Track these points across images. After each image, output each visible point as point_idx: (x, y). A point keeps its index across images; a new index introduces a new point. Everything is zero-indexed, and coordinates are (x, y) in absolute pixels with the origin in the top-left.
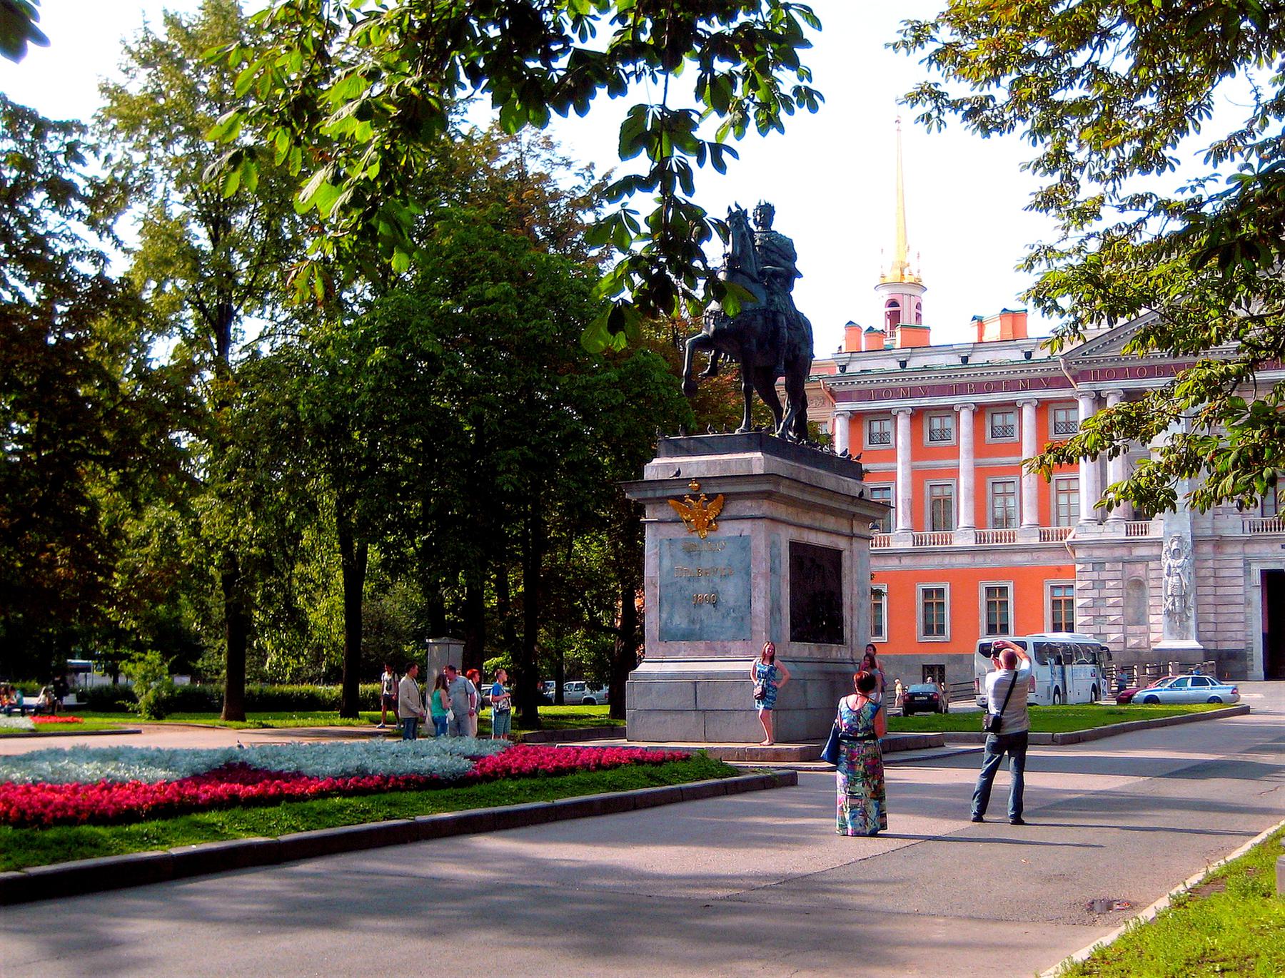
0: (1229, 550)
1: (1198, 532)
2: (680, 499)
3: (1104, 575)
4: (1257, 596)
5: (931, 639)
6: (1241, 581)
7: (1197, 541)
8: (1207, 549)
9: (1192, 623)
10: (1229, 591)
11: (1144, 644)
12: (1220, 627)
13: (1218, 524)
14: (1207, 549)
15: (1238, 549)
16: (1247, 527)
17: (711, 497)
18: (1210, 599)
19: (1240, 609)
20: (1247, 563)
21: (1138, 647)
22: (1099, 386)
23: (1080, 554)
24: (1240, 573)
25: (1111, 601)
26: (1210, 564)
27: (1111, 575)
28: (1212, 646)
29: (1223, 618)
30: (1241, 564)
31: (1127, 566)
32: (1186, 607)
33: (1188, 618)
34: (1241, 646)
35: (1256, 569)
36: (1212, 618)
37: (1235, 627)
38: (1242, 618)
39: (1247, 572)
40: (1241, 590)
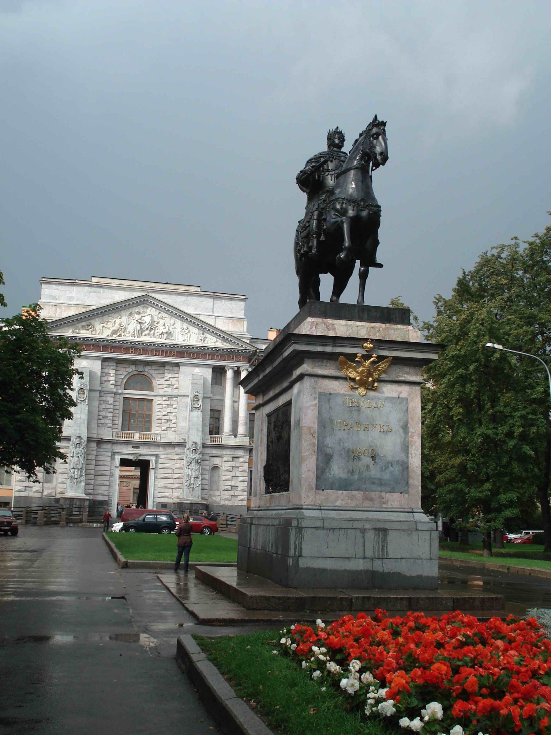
0: (104, 446)
1: (90, 436)
2: (351, 357)
6: (109, 464)
7: (89, 440)
10: (102, 468)
11: (53, 494)
13: (100, 432)
14: (94, 445)
15: (109, 446)
16: (114, 436)
17: (381, 358)
18: (93, 472)
21: (49, 495)
24: (109, 459)
28: (91, 497)
30: (110, 454)
34: (106, 498)
35: (117, 458)
36: (92, 482)
37: (104, 488)
38: (108, 484)
39: (113, 459)
40: (108, 468)
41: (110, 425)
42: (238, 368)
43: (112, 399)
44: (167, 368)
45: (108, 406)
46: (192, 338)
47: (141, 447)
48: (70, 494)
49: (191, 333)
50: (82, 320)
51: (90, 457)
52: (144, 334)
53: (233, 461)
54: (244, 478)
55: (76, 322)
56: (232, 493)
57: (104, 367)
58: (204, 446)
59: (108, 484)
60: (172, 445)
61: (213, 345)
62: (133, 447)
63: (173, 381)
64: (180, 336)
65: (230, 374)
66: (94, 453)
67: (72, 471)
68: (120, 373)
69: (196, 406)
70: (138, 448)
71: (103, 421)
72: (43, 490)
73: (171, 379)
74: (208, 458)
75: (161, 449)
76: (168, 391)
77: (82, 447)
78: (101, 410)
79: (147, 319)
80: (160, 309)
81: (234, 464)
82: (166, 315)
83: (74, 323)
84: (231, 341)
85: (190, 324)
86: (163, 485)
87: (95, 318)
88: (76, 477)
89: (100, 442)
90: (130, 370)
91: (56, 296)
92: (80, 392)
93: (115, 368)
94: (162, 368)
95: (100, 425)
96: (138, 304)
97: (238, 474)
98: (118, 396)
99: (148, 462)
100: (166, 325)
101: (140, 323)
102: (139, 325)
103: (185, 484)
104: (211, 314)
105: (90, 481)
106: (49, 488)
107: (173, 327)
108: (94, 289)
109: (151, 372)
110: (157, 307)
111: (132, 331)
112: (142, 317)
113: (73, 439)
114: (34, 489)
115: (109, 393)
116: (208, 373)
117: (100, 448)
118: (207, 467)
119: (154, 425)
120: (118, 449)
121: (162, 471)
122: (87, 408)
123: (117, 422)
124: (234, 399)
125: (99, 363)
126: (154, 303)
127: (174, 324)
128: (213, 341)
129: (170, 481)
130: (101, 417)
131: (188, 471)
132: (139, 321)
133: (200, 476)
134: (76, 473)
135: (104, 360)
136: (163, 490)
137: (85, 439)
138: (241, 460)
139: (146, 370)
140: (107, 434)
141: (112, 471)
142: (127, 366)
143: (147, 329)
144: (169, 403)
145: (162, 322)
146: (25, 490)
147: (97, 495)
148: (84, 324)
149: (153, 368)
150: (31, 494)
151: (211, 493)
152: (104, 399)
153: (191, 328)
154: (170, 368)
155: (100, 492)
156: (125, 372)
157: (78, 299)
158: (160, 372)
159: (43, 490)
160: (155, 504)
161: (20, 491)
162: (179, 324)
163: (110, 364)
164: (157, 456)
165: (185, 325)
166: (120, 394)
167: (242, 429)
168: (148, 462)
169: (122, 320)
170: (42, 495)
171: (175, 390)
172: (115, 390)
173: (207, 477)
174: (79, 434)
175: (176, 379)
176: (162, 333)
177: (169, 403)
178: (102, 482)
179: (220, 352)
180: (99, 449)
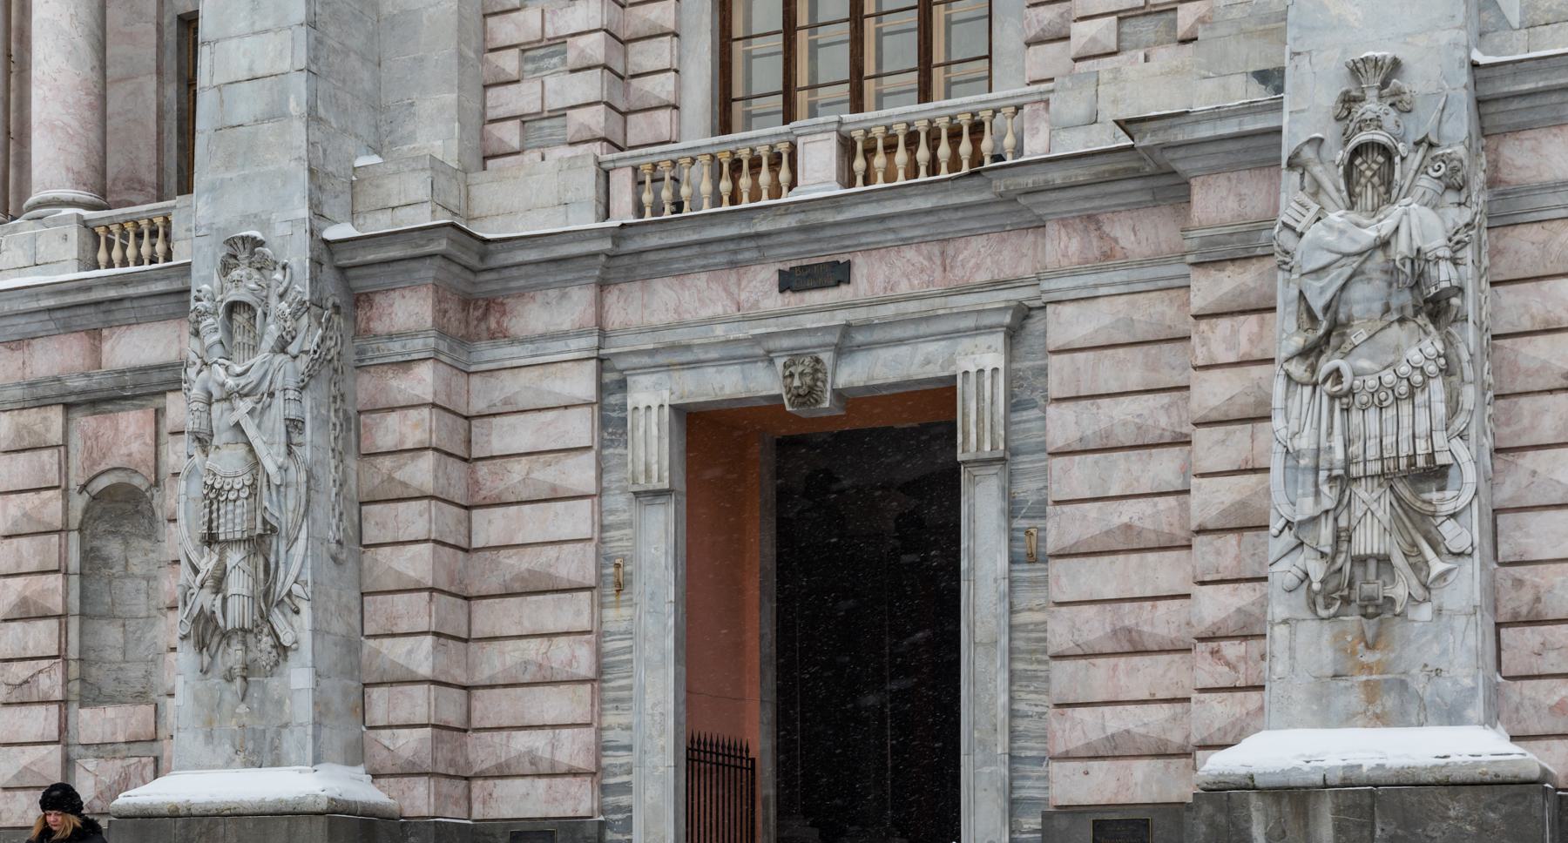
0: (533, 316)
4: (655, 541)
6: (580, 473)
10: (532, 523)
19: (574, 612)
24: (579, 428)
26: (423, 381)
29: (495, 662)
30: (582, 383)
35: (651, 398)
39: (612, 423)
40: (575, 520)
47: (861, 267)
62: (789, 282)
70: (839, 274)
99: (939, 399)
103: (1284, 572)
131: (1299, 421)
133: (1466, 459)
140: (539, 198)
141: (618, 543)
164: (1019, 326)
168: (939, 399)
174: (247, 219)
178: (533, 648)
180: (490, 354)
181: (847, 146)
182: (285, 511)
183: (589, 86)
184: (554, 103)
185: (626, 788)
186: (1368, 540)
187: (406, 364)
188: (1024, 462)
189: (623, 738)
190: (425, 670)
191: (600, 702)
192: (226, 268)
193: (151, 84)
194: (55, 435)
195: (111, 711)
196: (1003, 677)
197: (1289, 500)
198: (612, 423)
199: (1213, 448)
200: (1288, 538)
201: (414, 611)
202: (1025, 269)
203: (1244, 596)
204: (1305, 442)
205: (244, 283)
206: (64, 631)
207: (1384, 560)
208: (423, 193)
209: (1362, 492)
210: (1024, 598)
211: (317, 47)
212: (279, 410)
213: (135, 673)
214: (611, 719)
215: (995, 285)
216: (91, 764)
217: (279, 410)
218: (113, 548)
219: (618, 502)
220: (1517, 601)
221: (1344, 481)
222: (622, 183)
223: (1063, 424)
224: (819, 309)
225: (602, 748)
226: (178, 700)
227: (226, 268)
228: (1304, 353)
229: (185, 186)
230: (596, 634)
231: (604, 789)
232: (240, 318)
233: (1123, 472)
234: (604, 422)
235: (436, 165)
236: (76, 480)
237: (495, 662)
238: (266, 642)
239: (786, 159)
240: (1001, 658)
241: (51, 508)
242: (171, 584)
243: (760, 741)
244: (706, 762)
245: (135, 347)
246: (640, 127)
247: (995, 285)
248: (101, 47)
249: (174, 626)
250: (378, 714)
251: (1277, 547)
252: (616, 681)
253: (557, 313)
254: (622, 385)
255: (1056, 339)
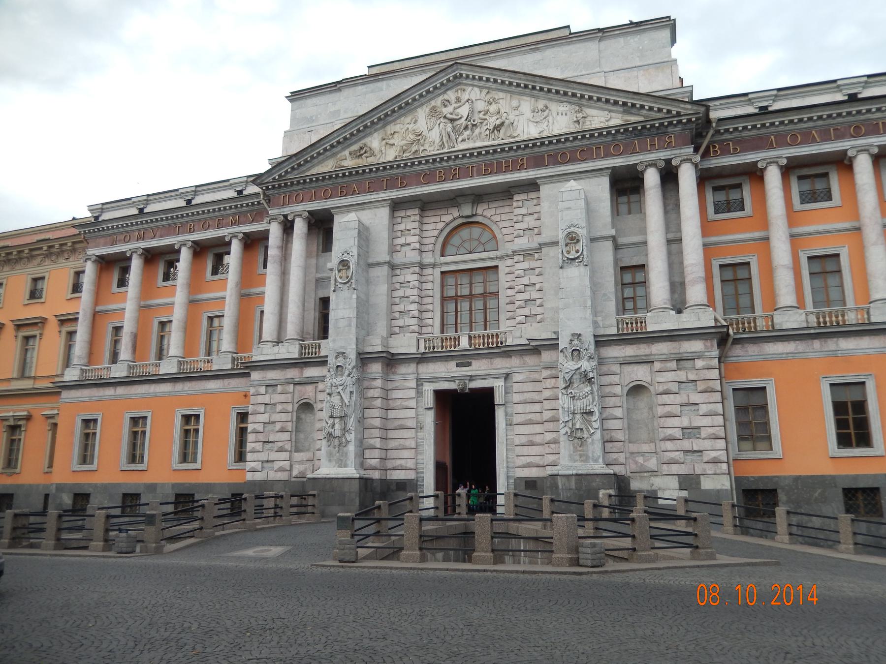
0: (403, 369)
3: (277, 398)
4: (429, 419)
5: (133, 467)
6: (412, 403)
7: (364, 359)
8: (376, 368)
9: (351, 448)
12: (392, 454)
14: (376, 368)
15: (411, 368)
19: (410, 433)
20: (420, 382)
21: (302, 475)
22: (286, 210)
23: (255, 375)
24: (412, 393)
25: (278, 426)
27: (282, 398)
28: (376, 475)
29: (392, 444)
30: (413, 384)
31: (298, 387)
32: (345, 430)
33: (348, 442)
34: (411, 475)
35: (429, 389)
37: (406, 454)
38: (413, 446)
39: (419, 393)
40: (411, 413)
41: (416, 328)
42: (668, 161)
43: (416, 277)
44: (516, 198)
45: (409, 292)
46: (560, 120)
47: (474, 363)
48: (327, 470)
49: (555, 114)
50: (348, 142)
51: (371, 393)
52: (460, 139)
53: (678, 369)
54: (711, 406)
55: (339, 148)
56: (686, 445)
57: (399, 220)
58: (601, 342)
59: (413, 446)
60: (534, 349)
61: (602, 125)
63: (530, 222)
64: (532, 125)
65: (652, 178)
66: (379, 383)
67: (330, 421)
68: (431, 227)
69: (573, 255)
70: (469, 364)
71: (400, 323)
72: (291, 466)
73: (527, 218)
74: (616, 368)
75: (515, 361)
76: (523, 243)
77: (347, 373)
78: (397, 300)
79: (464, 111)
80: (489, 84)
81: (682, 375)
82: (501, 95)
83: (335, 150)
84: (642, 107)
85: (551, 100)
86: (524, 439)
87: (370, 134)
88: (337, 433)
89: (391, 361)
90: (447, 218)
91: (311, 117)
92: (341, 267)
93: (417, 218)
94: (508, 202)
95: (397, 330)
96: (445, 87)
97: (695, 398)
98: (428, 271)
99: (490, 391)
100: (502, 111)
101: (452, 121)
102: (450, 125)
103: (563, 431)
104: (598, 70)
105: (372, 441)
106: (301, 462)
107: (517, 112)
108: (371, 86)
109: (488, 213)
110: (481, 83)
111: (437, 140)
112: (455, 109)
113: (331, 361)
114: (277, 465)
115: (406, 266)
116: (601, 188)
117: (394, 373)
118: (617, 390)
119: (502, 317)
120: (430, 369)
121: (519, 408)
122: (355, 296)
123: (430, 322)
124: (671, 236)
125: (384, 213)
126: (474, 77)
127: (517, 108)
128: (603, 119)
129: (538, 429)
130: (397, 315)
131: (564, 402)
132: (449, 116)
133: (596, 410)
134: (337, 427)
135: (396, 205)
136: (525, 450)
137: (353, 356)
138: (699, 363)
139: (479, 211)
140: (404, 344)
141: (421, 418)
142: (443, 212)
143: (466, 128)
144: (525, 265)
145: (493, 108)
146: (263, 467)
147: (394, 469)
148: (355, 147)
149: (492, 205)
150: (273, 476)
151: (633, 448)
152: (401, 279)
153: (554, 107)
154: (523, 197)
155: (398, 462)
156: (438, 223)
157: (345, 112)
158: (507, 209)
159: (291, 466)
160: (512, 481)
161: (254, 471)
162: (527, 105)
163: (409, 212)
164: (507, 377)
165: (541, 104)
166: (434, 266)
167: (696, 293)
168: (490, 391)
169: (418, 124)
170: (291, 475)
171: (536, 238)
172: (418, 259)
173: (618, 412)
174: (341, 347)
175: (536, 216)
176: (495, 128)
177: (525, 265)
178: (402, 442)
179: (620, 137)
180: (392, 377)
181: (470, 337)
182: (350, 411)
183: (414, 321)
184: (406, 324)
185: (422, 473)
186: (578, 426)
187: (374, 379)
188: (508, 405)
189: (422, 461)
190: (378, 446)
191: (417, 453)
192: (336, 357)
193: (313, 312)
194: (291, 390)
195: (302, 454)
196: (505, 450)
197: (564, 417)
198: (419, 393)
199: (548, 405)
200: (563, 424)
201: (376, 433)
202: (508, 365)
203: (555, 435)
204: (566, 406)
205: (340, 361)
206: (291, 435)
207: (582, 429)
208: (380, 343)
209: (578, 416)
210: (509, 433)
211: (358, 312)
212: (348, 389)
213: (307, 444)
214: (419, 457)
215: (502, 368)
216: (297, 466)
217: (348, 389)
218: (303, 416)
219: (421, 410)
220: (607, 437)
221: (573, 413)
222: (422, 342)
223: (516, 398)
224: (465, 371)
225: (417, 463)
226: (322, 452)
227: (336, 357)
228: (565, 388)
229: (326, 337)
230: (416, 438)
231: (417, 473)
232: (339, 369)
233: (529, 408)
234: (418, 392)
235: (382, 337)
236: (296, 401)
237: (392, 444)
238: (344, 440)
239: (457, 340)
240: (504, 446)
241: (289, 407)
242: (318, 425)
243: (448, 461)
244: (440, 467)
245: (311, 372)
246: (425, 330)
247: (502, 368)
248: (304, 305)
249: (322, 435)
250: (367, 456)
251: (561, 426)
252: (420, 449)
253: (407, 370)
254: (422, 385)
255: (515, 380)
